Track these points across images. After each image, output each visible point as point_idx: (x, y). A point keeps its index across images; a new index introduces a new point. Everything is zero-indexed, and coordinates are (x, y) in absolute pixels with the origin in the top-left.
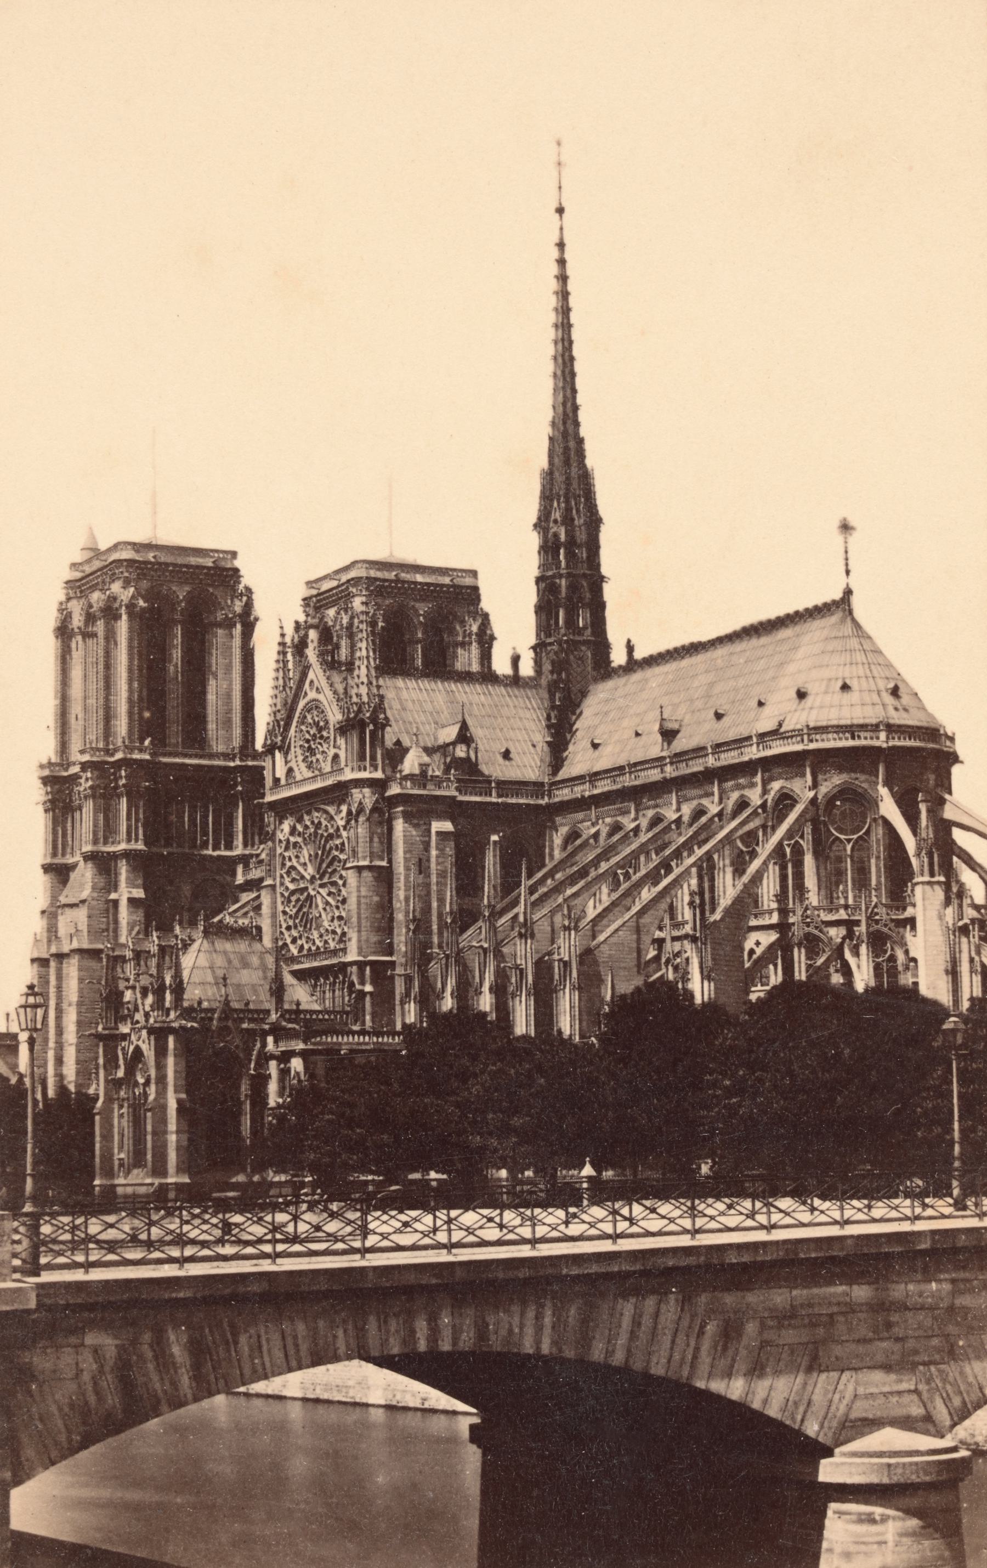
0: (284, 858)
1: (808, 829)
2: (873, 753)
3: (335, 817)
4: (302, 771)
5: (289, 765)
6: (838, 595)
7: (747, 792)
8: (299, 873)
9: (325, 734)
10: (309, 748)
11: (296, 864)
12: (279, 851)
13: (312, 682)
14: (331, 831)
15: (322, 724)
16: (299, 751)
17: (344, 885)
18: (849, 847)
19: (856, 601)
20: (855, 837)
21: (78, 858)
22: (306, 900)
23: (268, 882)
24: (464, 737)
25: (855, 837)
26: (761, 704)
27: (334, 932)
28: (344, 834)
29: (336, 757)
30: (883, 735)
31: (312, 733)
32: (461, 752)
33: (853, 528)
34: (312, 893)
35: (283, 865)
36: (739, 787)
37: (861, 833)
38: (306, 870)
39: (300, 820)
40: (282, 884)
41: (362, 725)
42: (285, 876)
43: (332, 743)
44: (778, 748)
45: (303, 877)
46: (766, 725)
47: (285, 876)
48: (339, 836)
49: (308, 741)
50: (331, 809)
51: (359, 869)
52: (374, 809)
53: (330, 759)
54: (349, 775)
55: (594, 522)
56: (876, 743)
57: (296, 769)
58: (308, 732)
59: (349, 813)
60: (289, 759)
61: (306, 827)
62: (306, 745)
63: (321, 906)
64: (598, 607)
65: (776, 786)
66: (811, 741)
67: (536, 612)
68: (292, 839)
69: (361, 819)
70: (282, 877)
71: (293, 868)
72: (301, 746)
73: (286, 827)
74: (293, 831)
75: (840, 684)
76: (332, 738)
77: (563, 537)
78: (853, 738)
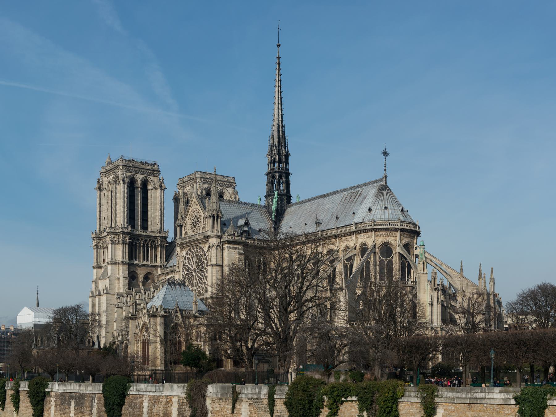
0: (184, 262)
1: (372, 256)
2: (396, 230)
3: (204, 249)
4: (190, 233)
5: (186, 231)
7: (348, 243)
8: (189, 268)
9: (199, 220)
10: (194, 225)
11: (188, 264)
12: (181, 260)
13: (195, 202)
14: (201, 253)
15: (198, 217)
16: (189, 226)
17: (207, 271)
18: (386, 262)
19: (388, 179)
20: (388, 259)
21: (105, 264)
22: (192, 276)
23: (178, 270)
25: (388, 259)
26: (354, 213)
27: (203, 288)
28: (207, 254)
29: (204, 228)
30: (399, 225)
31: (194, 220)
32: (246, 229)
34: (194, 274)
35: (184, 265)
36: (345, 241)
37: (390, 258)
38: (192, 267)
39: (190, 250)
40: (183, 271)
41: (214, 216)
42: (184, 268)
43: (202, 223)
44: (361, 227)
45: (190, 269)
46: (357, 219)
47: (184, 268)
48: (205, 255)
50: (202, 246)
51: (212, 265)
52: (218, 246)
53: (201, 228)
54: (209, 234)
55: (287, 156)
56: (397, 227)
57: (188, 232)
58: (193, 219)
59: (209, 246)
60: (186, 228)
61: (192, 252)
62: (192, 224)
63: (197, 278)
64: (288, 184)
65: (360, 241)
66: (375, 225)
67: (267, 185)
68: (186, 256)
69: (214, 248)
70: (182, 268)
72: (190, 224)
73: (184, 252)
74: (187, 254)
75: (384, 207)
76: (202, 221)
77: (277, 160)
78: (389, 224)
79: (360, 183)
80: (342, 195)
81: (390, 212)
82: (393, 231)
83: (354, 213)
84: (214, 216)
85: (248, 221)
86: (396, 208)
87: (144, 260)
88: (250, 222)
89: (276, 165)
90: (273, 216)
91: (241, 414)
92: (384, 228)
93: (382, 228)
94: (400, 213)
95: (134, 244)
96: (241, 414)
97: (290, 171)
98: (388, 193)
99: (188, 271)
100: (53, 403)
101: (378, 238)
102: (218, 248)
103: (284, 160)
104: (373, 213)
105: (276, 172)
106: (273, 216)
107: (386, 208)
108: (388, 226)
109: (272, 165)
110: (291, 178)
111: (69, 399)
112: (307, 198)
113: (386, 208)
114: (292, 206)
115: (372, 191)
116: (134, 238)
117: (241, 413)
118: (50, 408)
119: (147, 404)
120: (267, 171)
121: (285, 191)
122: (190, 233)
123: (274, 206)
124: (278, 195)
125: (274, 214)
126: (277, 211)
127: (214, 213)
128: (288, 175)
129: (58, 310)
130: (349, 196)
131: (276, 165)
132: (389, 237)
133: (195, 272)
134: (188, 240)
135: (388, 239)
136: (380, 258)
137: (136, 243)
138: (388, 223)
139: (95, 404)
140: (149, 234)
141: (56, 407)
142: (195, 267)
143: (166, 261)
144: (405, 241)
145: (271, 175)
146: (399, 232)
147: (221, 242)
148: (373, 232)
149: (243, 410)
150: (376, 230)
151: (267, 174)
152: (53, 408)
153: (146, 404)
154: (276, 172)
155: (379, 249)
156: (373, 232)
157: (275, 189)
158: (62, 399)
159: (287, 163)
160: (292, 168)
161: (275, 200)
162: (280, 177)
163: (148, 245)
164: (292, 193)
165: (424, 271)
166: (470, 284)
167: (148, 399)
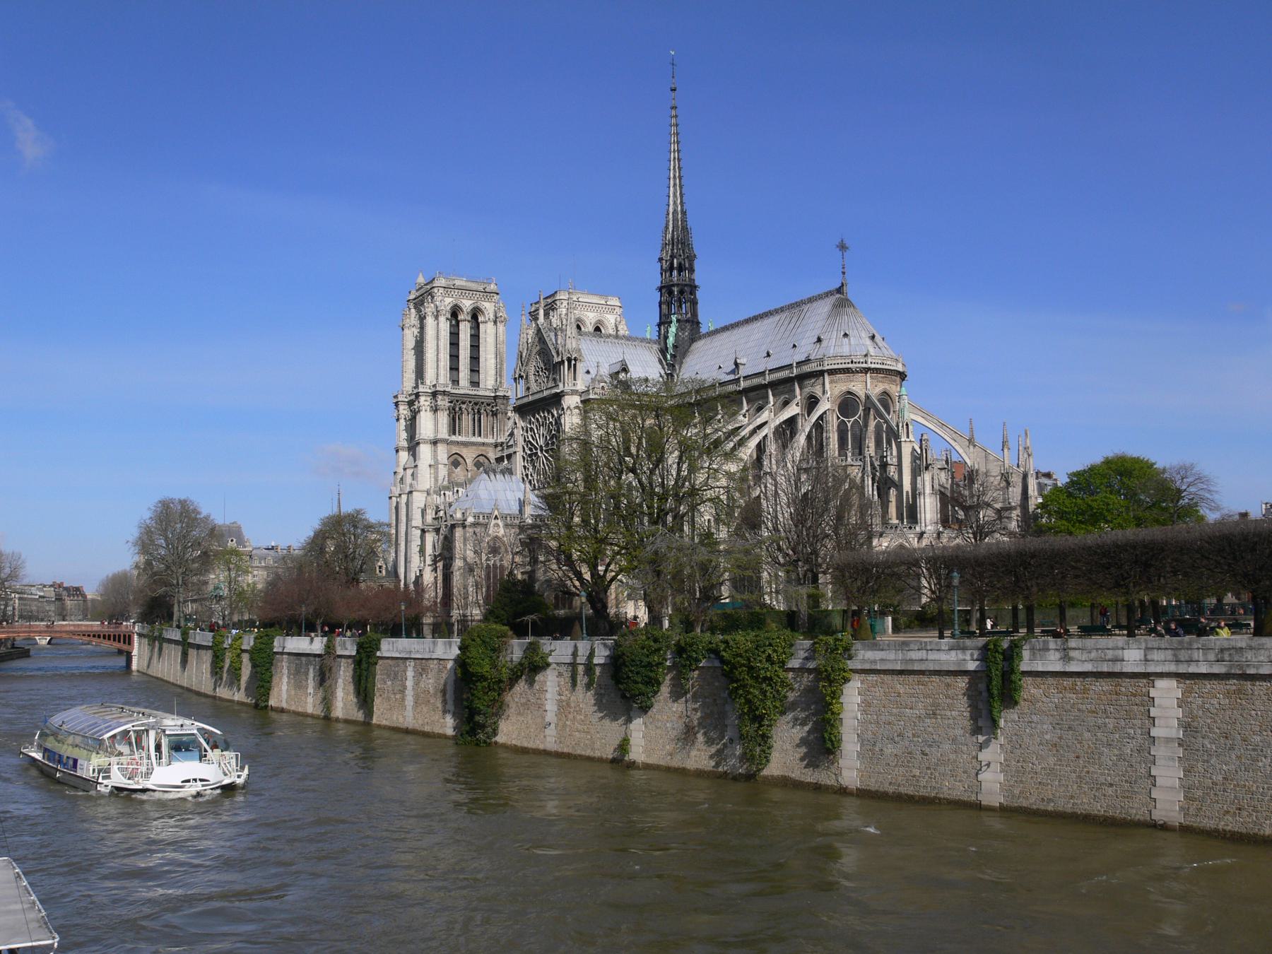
6: (838, 286)
8: (532, 444)
20: (852, 419)
24: (625, 370)
25: (852, 419)
26: (794, 346)
32: (622, 376)
33: (847, 248)
35: (525, 441)
49: (538, 372)
55: (691, 258)
56: (864, 365)
61: (537, 419)
64: (694, 303)
71: (529, 441)
75: (842, 333)
78: (852, 362)
79: (805, 296)
80: (777, 318)
81: (852, 342)
82: (857, 372)
83: (794, 346)
84: (569, 360)
85: (626, 365)
86: (863, 334)
87: (474, 435)
88: (629, 367)
89: (675, 273)
90: (669, 356)
91: (546, 691)
92: (843, 369)
93: (839, 369)
94: (868, 342)
95: (457, 409)
96: (546, 691)
97: (697, 283)
98: (850, 310)
99: (531, 450)
100: (285, 671)
101: (834, 385)
102: (577, 411)
103: (687, 265)
104: (824, 343)
105: (673, 285)
106: (669, 356)
107: (846, 335)
108: (850, 366)
109: (668, 274)
110: (699, 294)
111: (307, 665)
112: (723, 325)
113: (846, 335)
114: (700, 338)
115: (824, 307)
116: (457, 401)
117: (545, 689)
118: (281, 679)
119: (413, 674)
120: (659, 284)
121: (689, 315)
122: (534, 388)
123: (671, 340)
124: (678, 321)
125: (671, 351)
126: (675, 347)
127: (569, 355)
128: (693, 288)
129: (327, 518)
130: (788, 319)
131: (675, 273)
132: (853, 384)
133: (541, 450)
134: (531, 398)
135: (851, 386)
136: (838, 418)
137: (460, 409)
138: (850, 361)
139: (341, 673)
140: (480, 393)
141: (289, 677)
142: (541, 442)
143: (509, 436)
144: (880, 388)
145: (666, 289)
146: (868, 375)
147: (581, 401)
148: (826, 375)
149: (548, 683)
150: (832, 372)
151: (660, 289)
152: (285, 680)
153: (410, 673)
154: (673, 285)
155: (838, 403)
156: (826, 375)
157: (673, 312)
158: (296, 665)
159: (692, 270)
160: (698, 277)
161: (673, 329)
162: (681, 292)
163: (479, 412)
164: (701, 318)
165: (908, 437)
166: (991, 458)
167: (412, 664)
